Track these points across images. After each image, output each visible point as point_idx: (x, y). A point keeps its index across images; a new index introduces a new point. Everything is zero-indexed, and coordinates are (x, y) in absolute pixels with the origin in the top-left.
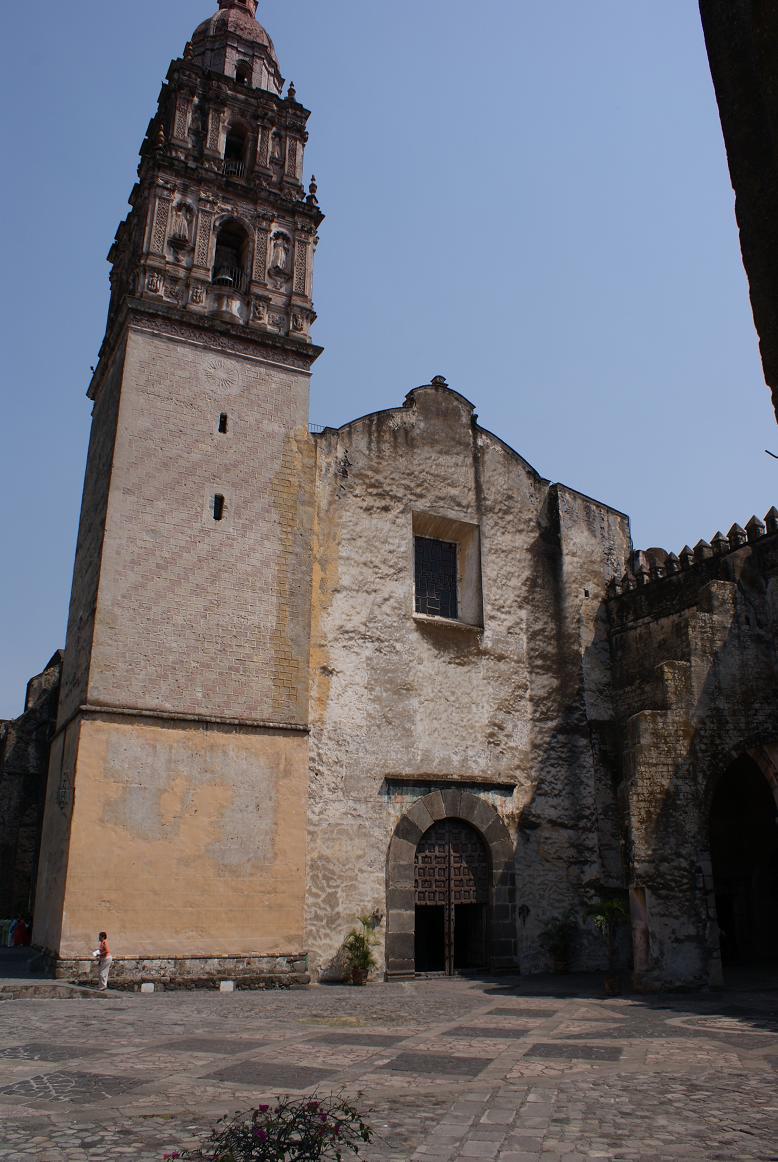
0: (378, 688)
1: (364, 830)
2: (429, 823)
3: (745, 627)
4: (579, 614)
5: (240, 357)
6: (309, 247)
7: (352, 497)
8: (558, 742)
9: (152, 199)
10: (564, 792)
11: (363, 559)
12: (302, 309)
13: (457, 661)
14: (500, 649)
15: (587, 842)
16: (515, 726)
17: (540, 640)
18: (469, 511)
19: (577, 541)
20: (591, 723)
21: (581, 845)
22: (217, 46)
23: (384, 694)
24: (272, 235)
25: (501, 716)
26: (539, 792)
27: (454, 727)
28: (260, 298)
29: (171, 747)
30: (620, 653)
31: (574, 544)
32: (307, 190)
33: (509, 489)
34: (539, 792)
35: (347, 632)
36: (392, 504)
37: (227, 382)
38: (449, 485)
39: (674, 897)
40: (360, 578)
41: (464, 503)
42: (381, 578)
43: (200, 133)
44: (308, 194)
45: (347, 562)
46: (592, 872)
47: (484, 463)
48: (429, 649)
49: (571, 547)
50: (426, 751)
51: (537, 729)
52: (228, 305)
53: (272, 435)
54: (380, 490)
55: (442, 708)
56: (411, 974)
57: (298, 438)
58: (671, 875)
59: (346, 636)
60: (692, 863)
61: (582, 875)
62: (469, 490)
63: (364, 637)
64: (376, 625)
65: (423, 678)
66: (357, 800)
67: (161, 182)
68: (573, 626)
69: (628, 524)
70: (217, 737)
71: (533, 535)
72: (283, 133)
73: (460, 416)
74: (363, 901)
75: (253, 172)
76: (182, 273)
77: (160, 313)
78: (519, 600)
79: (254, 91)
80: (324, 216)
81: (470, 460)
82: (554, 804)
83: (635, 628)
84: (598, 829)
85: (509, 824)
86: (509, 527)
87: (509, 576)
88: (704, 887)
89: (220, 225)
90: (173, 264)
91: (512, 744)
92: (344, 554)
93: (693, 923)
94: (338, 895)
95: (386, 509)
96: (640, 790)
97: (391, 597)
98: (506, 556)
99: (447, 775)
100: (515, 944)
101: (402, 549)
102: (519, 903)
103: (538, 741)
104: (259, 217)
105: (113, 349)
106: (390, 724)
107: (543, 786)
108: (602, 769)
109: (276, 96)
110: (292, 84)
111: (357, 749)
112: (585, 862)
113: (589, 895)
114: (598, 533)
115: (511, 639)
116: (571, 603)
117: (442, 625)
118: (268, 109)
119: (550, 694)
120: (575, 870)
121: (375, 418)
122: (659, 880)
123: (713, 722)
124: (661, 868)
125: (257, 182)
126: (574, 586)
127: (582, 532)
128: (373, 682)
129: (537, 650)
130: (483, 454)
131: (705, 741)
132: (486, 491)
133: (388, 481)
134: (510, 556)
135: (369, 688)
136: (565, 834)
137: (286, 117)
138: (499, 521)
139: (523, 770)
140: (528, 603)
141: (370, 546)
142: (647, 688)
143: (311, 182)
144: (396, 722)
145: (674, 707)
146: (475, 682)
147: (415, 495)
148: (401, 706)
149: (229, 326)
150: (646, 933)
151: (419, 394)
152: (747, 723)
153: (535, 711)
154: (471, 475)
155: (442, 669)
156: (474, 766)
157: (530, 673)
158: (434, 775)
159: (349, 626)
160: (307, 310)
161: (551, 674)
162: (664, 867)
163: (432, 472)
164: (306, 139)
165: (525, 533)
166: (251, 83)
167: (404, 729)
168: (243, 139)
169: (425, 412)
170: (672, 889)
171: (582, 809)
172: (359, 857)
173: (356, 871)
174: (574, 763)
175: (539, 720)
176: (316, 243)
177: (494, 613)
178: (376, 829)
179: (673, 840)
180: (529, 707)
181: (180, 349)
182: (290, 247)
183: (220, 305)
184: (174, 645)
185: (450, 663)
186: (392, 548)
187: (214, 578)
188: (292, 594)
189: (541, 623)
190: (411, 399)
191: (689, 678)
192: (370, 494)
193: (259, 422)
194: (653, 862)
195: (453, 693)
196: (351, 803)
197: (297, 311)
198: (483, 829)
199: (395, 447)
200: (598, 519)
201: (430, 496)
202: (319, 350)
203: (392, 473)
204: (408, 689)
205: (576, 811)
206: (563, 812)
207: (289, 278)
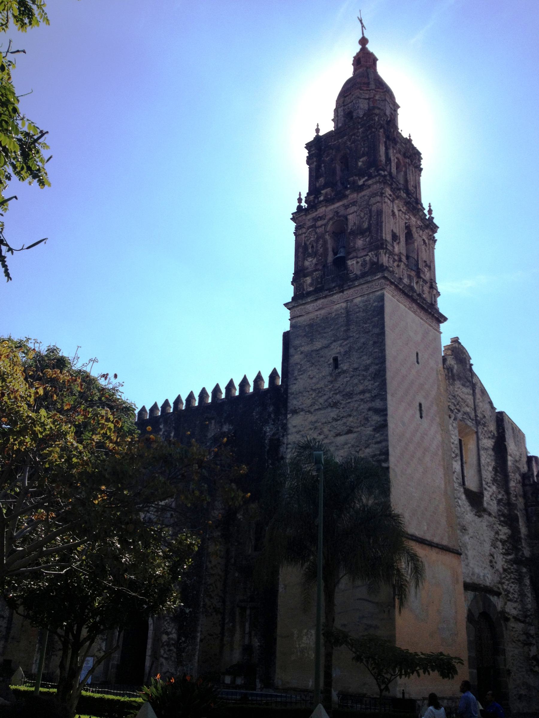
4: (516, 492)
8: (513, 569)
16: (497, 556)
17: (501, 505)
25: (493, 550)
41: (472, 417)
51: (504, 559)
61: (530, 652)
77: (396, 283)
81: (471, 392)
99: (480, 584)
103: (505, 567)
107: (510, 595)
116: (512, 484)
132: (477, 411)
136: (521, 625)
153: (503, 549)
154: (472, 401)
156: (487, 580)
202: (445, 319)
204: (464, 530)
206: (519, 612)
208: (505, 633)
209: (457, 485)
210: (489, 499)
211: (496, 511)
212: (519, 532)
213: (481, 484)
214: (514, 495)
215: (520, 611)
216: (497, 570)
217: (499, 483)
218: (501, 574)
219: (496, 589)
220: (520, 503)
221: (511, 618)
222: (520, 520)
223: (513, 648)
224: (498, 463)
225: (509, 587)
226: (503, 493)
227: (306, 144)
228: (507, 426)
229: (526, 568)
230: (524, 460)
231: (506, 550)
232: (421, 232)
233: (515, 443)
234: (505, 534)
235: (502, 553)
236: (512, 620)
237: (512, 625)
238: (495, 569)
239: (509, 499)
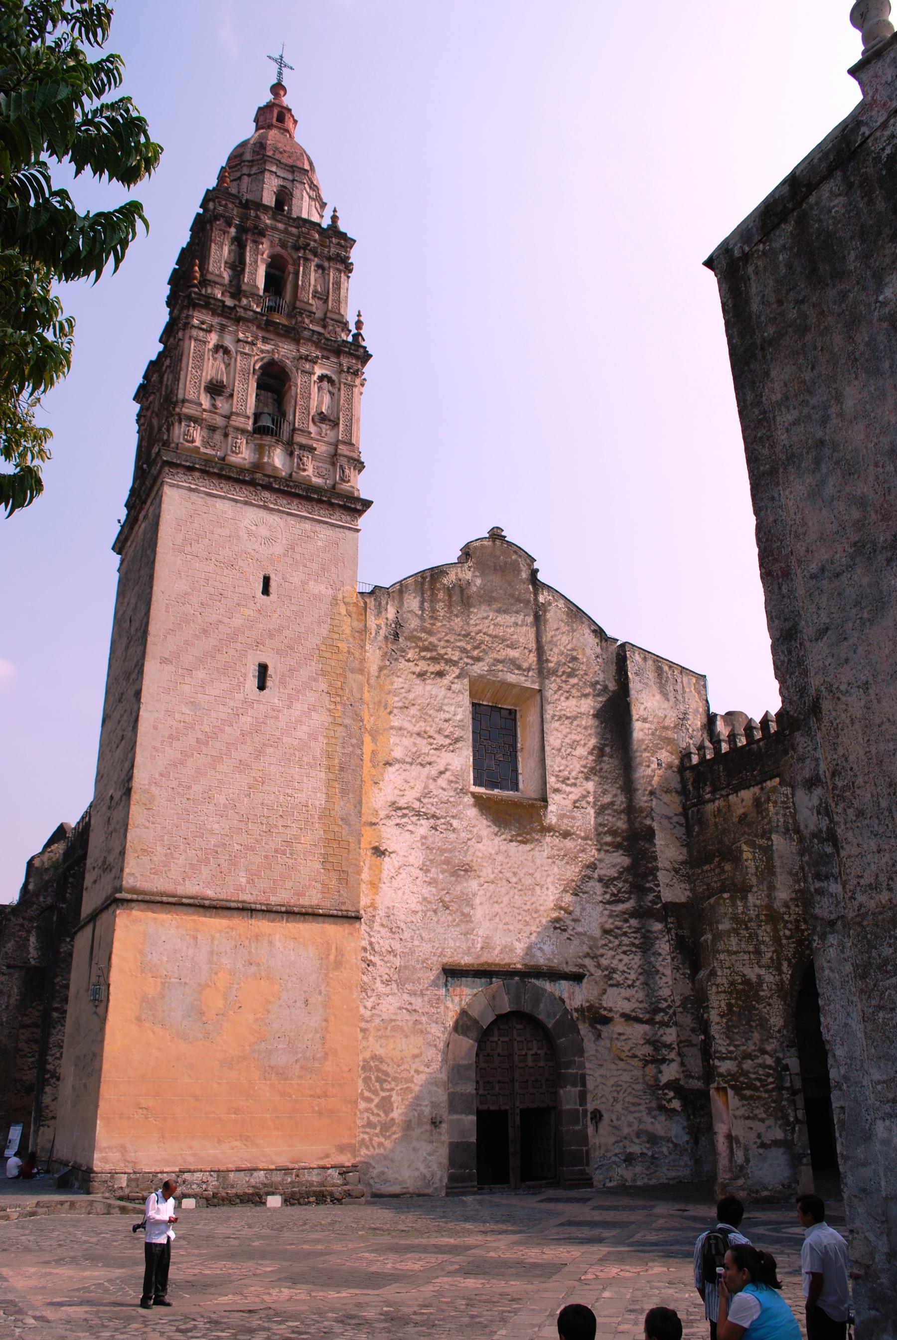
0: (433, 870)
1: (420, 1026)
2: (491, 1018)
4: (651, 785)
5: (283, 512)
6: (356, 390)
7: (403, 661)
8: (630, 927)
9: (187, 341)
10: (638, 983)
11: (416, 729)
12: (350, 459)
13: (519, 838)
14: (565, 824)
15: (664, 1038)
16: (583, 909)
17: (609, 815)
18: (531, 674)
19: (649, 705)
20: (668, 906)
21: (658, 1041)
22: (254, 170)
23: (441, 876)
24: (315, 378)
26: (611, 982)
27: (517, 911)
28: (302, 447)
29: (213, 938)
30: (696, 829)
31: (645, 709)
32: (352, 327)
33: (573, 649)
34: (611, 982)
35: (400, 809)
36: (447, 668)
37: (270, 540)
38: (508, 646)
39: (759, 1098)
40: (414, 750)
41: (525, 665)
42: (436, 749)
43: (238, 266)
44: (354, 331)
45: (400, 732)
46: (670, 1072)
47: (546, 621)
48: (489, 826)
49: (642, 712)
50: (487, 938)
51: (606, 912)
52: (269, 457)
53: (318, 598)
54: (434, 653)
55: (503, 890)
56: (473, 1187)
57: (347, 600)
58: (754, 1073)
59: (400, 813)
60: (778, 1061)
61: (660, 1075)
62: (530, 651)
63: (418, 814)
64: (431, 800)
65: (482, 858)
66: (413, 993)
67: (196, 322)
68: (645, 798)
69: (705, 686)
70: (262, 925)
71: (600, 699)
72: (326, 264)
73: (519, 571)
74: (421, 1105)
75: (295, 308)
76: (219, 421)
77: (197, 466)
78: (586, 770)
79: (294, 219)
80: (371, 356)
81: (530, 619)
82: (627, 996)
84: (676, 1024)
85: (578, 1019)
86: (574, 691)
87: (574, 745)
88: (792, 1087)
89: (260, 368)
90: (210, 412)
91: (580, 929)
92: (396, 724)
93: (780, 1127)
94: (393, 1099)
95: (440, 674)
96: (719, 980)
97: (446, 770)
98: (571, 723)
99: (509, 964)
100: (587, 1152)
101: (458, 717)
102: (590, 1107)
103: (608, 926)
104: (301, 358)
105: (145, 502)
106: (448, 908)
107: (615, 976)
108: (679, 956)
109: (319, 225)
110: (335, 211)
111: (412, 938)
112: (664, 1061)
113: (668, 1097)
114: (671, 696)
115: (577, 814)
117: (502, 800)
118: (310, 239)
119: (621, 873)
120: (651, 1069)
121: (428, 574)
122: (742, 1079)
123: (797, 906)
124: (745, 1066)
125: (300, 319)
126: (646, 754)
127: (654, 696)
128: (428, 863)
129: (604, 825)
130: (545, 612)
131: (789, 926)
132: (548, 653)
133: (442, 643)
134: (575, 723)
135: (424, 869)
136: (640, 1029)
137: (329, 247)
138: (563, 685)
139: (593, 958)
140: (595, 774)
141: (424, 715)
142: (728, 867)
143: (356, 319)
144: (454, 906)
145: (755, 889)
146: (538, 862)
147: (472, 658)
148: (459, 888)
149: (271, 480)
150: (729, 1137)
151: (475, 548)
154: (532, 636)
155: (503, 848)
156: (539, 954)
157: (599, 850)
158: (496, 965)
159: (402, 802)
160: (355, 460)
161: (621, 852)
162: (748, 1065)
163: (490, 632)
164: (351, 271)
165: (591, 697)
166: (291, 210)
167: (463, 914)
168: (284, 272)
169: (482, 567)
170: (756, 1089)
171: (658, 1002)
172: (415, 1056)
173: (412, 1072)
174: (648, 950)
175: (609, 903)
176: (362, 385)
177: (558, 785)
178: (434, 1025)
179: (756, 1035)
180: (599, 888)
181: (220, 504)
182: (335, 391)
183: (261, 455)
184: (216, 826)
185: (511, 841)
186: (447, 716)
187: (259, 753)
188: (342, 769)
189: (610, 796)
190: (467, 553)
192: (424, 658)
193: (304, 583)
194: (735, 1059)
195: (515, 874)
196: (406, 997)
197: (343, 461)
198: (550, 1024)
199: (450, 606)
200: (672, 681)
201: (488, 659)
202: (367, 504)
203: (446, 634)
204: (466, 871)
205: (652, 1003)
206: (637, 1005)
207: (335, 424)
209: (452, 793)
213: (544, 782)
214: (647, 792)
218: (594, 939)
223: (618, 1070)
226: (619, 791)
227: (169, 284)
231: (613, 895)
232: (308, 366)
234: (614, 866)
235: (601, 902)
237: (619, 1029)
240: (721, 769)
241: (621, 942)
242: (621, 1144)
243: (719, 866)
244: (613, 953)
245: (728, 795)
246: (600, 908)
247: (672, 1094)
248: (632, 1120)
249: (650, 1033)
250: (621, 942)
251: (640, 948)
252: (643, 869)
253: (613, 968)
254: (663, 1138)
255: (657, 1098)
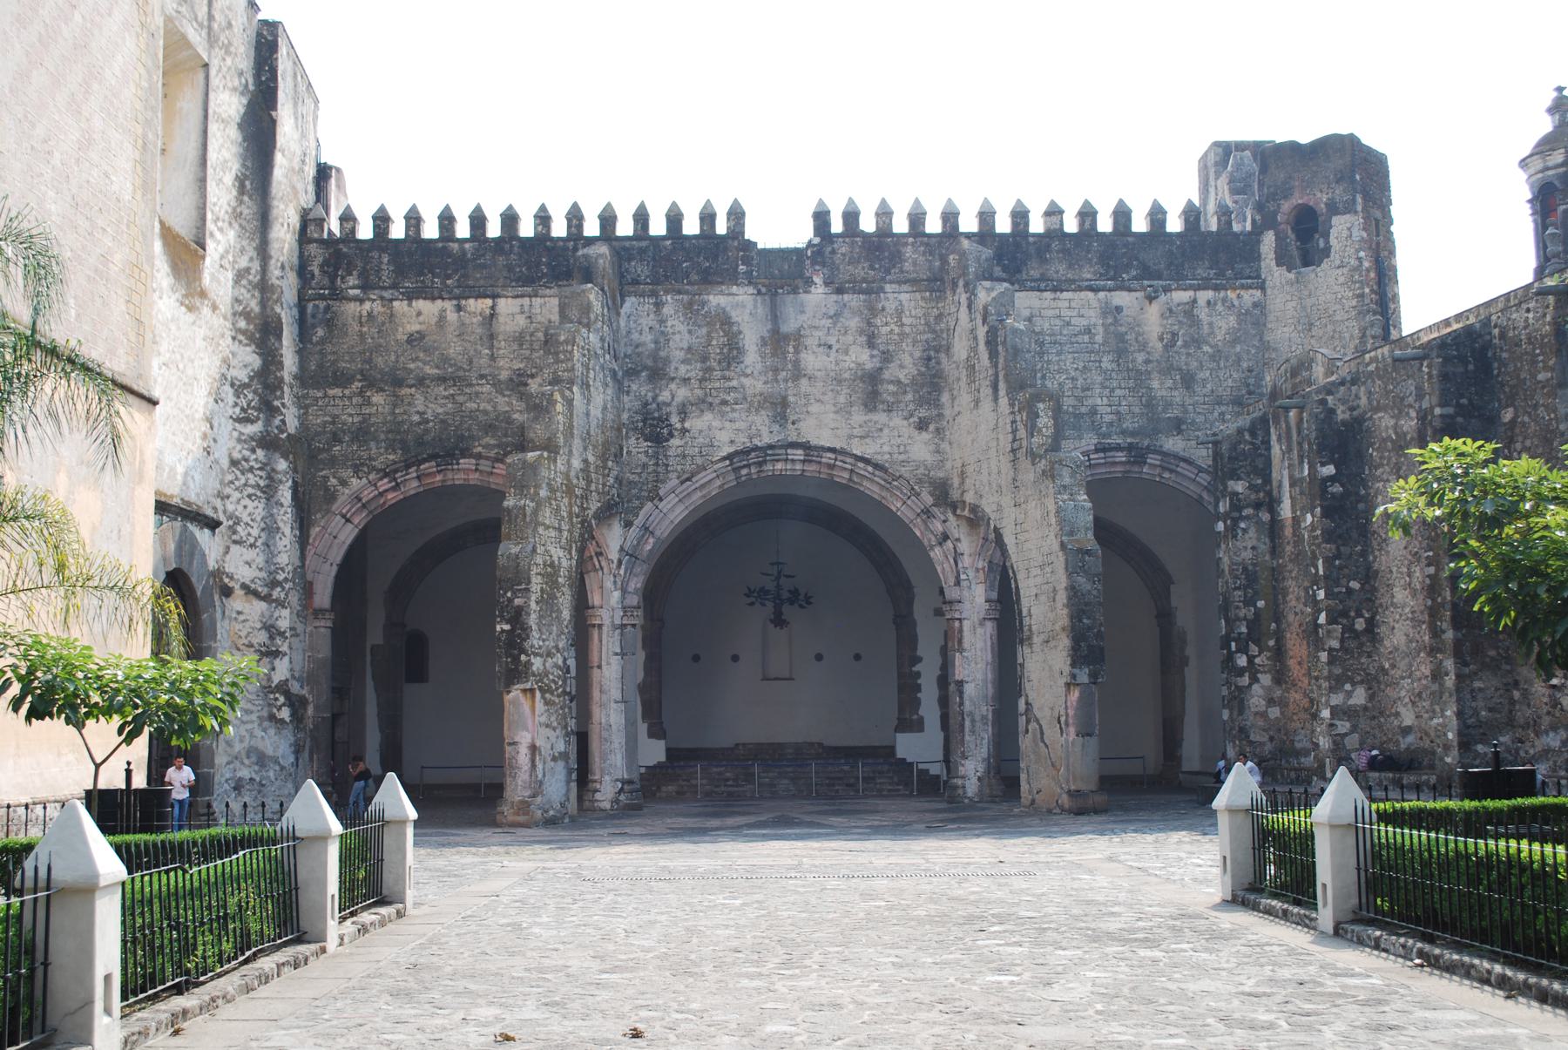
3: (607, 356)
8: (256, 460)
21: (273, 626)
26: (234, 537)
30: (320, 332)
33: (229, 8)
41: (200, 19)
51: (235, 434)
83: (362, 301)
103: (237, 456)
107: (239, 529)
112: (276, 654)
113: (279, 703)
119: (251, 378)
136: (260, 606)
139: (222, 499)
150: (533, 749)
152: (604, 485)
153: (236, 404)
156: (192, 486)
161: (253, 347)
175: (239, 420)
191: (572, 415)
208: (219, 625)
210: (217, 266)
211: (228, 300)
212: (280, 366)
213: (203, 219)
215: (261, 570)
216: (216, 462)
217: (244, 223)
218: (222, 469)
219: (209, 512)
220: (288, 286)
221: (237, 587)
222: (285, 333)
224: (247, 168)
225: (240, 508)
228: (283, 64)
229: (286, 459)
230: (311, 172)
231: (243, 409)
233: (296, 118)
234: (245, 366)
236: (239, 592)
238: (212, 458)
239: (264, 270)
240: (385, 260)
241: (247, 480)
242: (231, 766)
243: (361, 393)
244: (239, 496)
245: (391, 300)
246: (230, 424)
247: (282, 699)
248: (244, 733)
249: (267, 614)
250: (247, 480)
251: (264, 492)
252: (271, 379)
253: (237, 518)
254: (271, 758)
255: (269, 705)
